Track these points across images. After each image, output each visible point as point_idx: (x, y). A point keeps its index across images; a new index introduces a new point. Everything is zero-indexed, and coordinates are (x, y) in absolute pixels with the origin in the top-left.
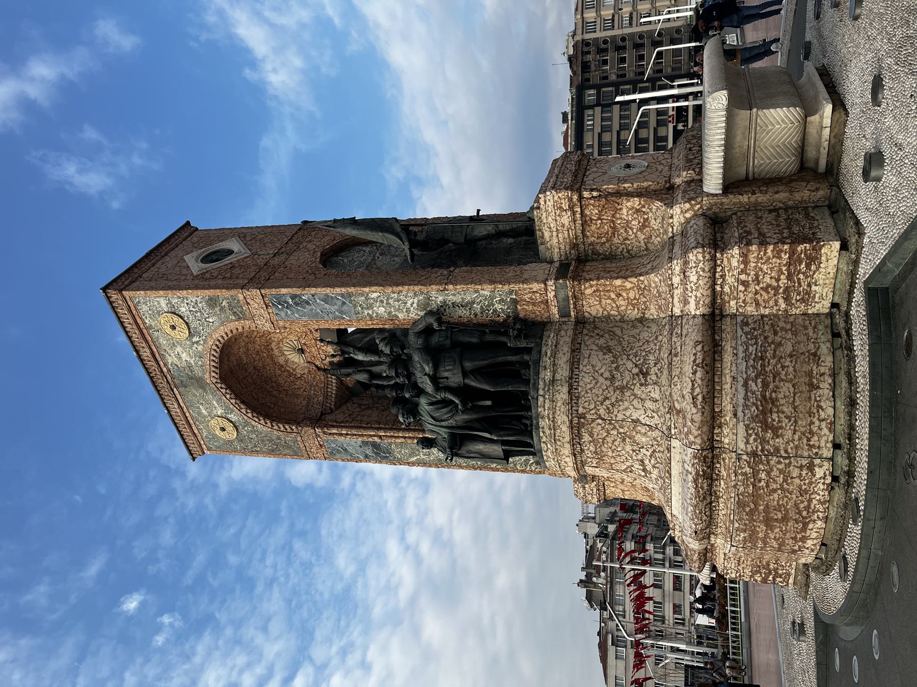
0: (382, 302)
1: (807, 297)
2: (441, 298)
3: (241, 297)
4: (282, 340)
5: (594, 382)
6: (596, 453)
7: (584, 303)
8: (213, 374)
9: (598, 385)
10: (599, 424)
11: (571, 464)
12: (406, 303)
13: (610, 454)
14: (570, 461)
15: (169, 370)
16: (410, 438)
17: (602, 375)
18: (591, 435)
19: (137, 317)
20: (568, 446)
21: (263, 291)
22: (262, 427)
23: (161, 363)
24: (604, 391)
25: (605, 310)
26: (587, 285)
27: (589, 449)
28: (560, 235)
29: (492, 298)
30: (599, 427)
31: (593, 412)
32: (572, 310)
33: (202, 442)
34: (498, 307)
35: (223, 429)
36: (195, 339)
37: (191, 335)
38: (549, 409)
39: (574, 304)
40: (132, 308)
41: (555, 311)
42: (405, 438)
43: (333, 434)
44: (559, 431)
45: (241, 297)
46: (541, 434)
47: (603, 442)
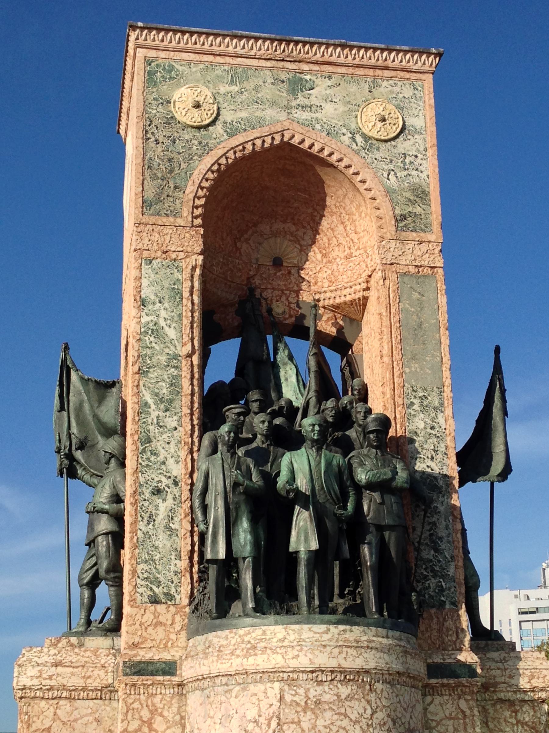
0: (432, 428)
2: (442, 508)
3: (432, 237)
4: (298, 241)
5: (405, 707)
6: (318, 703)
7: (446, 698)
9: (404, 712)
10: (365, 710)
11: (294, 664)
12: (432, 458)
14: (304, 662)
16: (192, 402)
17: (411, 717)
18: (349, 698)
19: (393, 73)
20: (333, 664)
21: (440, 271)
23: (316, 68)
24: (400, 718)
25: (438, 724)
27: (327, 693)
28: (499, 672)
29: (443, 577)
30: (361, 711)
31: (379, 703)
32: (439, 680)
33: (162, 54)
34: (432, 583)
35: (197, 106)
36: (359, 138)
37: (366, 138)
38: (381, 643)
39: (448, 685)
40: (408, 75)
41: (437, 659)
42: (192, 395)
43: (192, 281)
44: (355, 653)
45: (432, 237)
46: (341, 627)
47: (340, 714)
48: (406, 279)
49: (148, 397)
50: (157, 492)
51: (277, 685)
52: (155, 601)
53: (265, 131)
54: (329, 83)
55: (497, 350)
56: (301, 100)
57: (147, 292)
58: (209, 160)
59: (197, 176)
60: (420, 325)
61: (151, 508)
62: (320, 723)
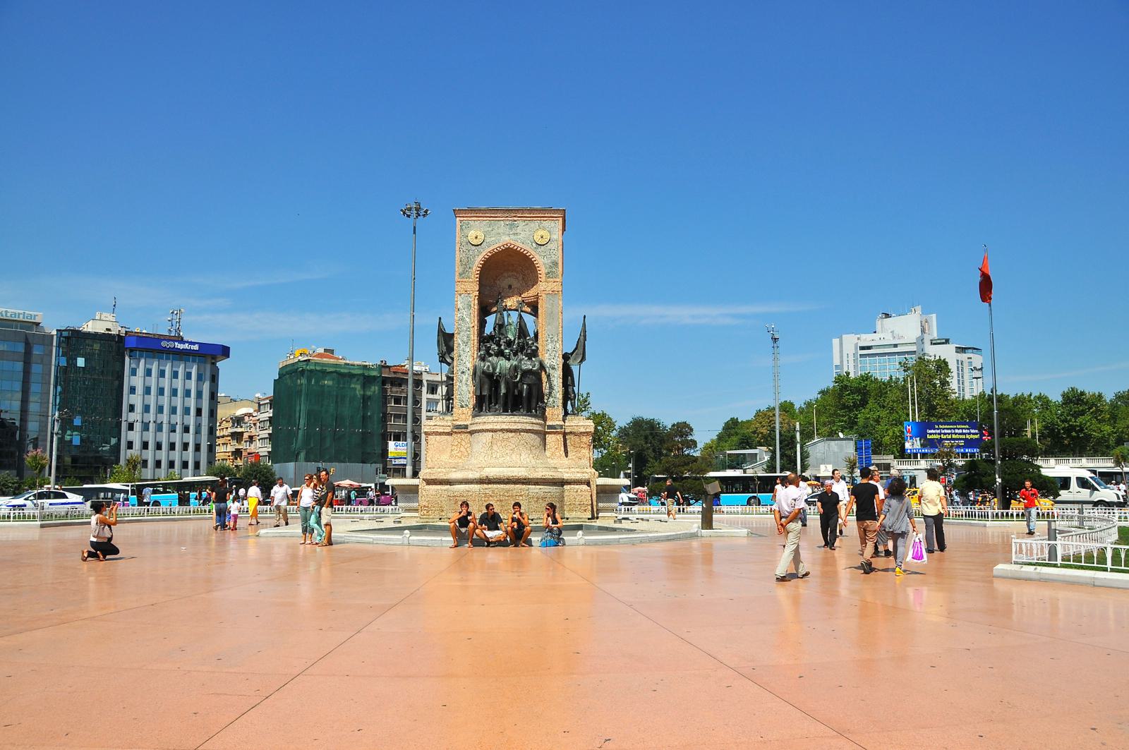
1: (570, 510)
2: (556, 375)
3: (558, 280)
8: (512, 246)
11: (495, 427)
13: (503, 444)
15: (515, 221)
18: (512, 437)
20: (507, 427)
22: (478, 262)
26: (562, 437)
33: (465, 219)
35: (476, 238)
36: (534, 245)
48: (548, 296)
49: (460, 342)
50: (463, 372)
51: (491, 433)
52: (462, 407)
53: (501, 244)
54: (524, 224)
55: (585, 317)
56: (514, 231)
57: (460, 306)
58: (481, 257)
59: (477, 263)
60: (552, 313)
61: (461, 378)
62: (503, 444)
